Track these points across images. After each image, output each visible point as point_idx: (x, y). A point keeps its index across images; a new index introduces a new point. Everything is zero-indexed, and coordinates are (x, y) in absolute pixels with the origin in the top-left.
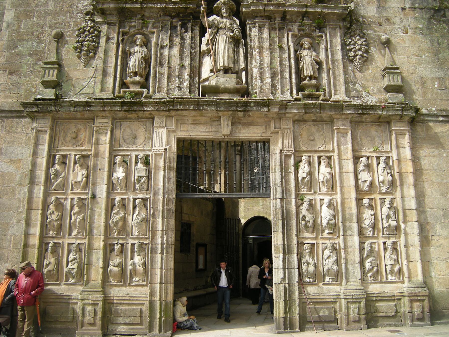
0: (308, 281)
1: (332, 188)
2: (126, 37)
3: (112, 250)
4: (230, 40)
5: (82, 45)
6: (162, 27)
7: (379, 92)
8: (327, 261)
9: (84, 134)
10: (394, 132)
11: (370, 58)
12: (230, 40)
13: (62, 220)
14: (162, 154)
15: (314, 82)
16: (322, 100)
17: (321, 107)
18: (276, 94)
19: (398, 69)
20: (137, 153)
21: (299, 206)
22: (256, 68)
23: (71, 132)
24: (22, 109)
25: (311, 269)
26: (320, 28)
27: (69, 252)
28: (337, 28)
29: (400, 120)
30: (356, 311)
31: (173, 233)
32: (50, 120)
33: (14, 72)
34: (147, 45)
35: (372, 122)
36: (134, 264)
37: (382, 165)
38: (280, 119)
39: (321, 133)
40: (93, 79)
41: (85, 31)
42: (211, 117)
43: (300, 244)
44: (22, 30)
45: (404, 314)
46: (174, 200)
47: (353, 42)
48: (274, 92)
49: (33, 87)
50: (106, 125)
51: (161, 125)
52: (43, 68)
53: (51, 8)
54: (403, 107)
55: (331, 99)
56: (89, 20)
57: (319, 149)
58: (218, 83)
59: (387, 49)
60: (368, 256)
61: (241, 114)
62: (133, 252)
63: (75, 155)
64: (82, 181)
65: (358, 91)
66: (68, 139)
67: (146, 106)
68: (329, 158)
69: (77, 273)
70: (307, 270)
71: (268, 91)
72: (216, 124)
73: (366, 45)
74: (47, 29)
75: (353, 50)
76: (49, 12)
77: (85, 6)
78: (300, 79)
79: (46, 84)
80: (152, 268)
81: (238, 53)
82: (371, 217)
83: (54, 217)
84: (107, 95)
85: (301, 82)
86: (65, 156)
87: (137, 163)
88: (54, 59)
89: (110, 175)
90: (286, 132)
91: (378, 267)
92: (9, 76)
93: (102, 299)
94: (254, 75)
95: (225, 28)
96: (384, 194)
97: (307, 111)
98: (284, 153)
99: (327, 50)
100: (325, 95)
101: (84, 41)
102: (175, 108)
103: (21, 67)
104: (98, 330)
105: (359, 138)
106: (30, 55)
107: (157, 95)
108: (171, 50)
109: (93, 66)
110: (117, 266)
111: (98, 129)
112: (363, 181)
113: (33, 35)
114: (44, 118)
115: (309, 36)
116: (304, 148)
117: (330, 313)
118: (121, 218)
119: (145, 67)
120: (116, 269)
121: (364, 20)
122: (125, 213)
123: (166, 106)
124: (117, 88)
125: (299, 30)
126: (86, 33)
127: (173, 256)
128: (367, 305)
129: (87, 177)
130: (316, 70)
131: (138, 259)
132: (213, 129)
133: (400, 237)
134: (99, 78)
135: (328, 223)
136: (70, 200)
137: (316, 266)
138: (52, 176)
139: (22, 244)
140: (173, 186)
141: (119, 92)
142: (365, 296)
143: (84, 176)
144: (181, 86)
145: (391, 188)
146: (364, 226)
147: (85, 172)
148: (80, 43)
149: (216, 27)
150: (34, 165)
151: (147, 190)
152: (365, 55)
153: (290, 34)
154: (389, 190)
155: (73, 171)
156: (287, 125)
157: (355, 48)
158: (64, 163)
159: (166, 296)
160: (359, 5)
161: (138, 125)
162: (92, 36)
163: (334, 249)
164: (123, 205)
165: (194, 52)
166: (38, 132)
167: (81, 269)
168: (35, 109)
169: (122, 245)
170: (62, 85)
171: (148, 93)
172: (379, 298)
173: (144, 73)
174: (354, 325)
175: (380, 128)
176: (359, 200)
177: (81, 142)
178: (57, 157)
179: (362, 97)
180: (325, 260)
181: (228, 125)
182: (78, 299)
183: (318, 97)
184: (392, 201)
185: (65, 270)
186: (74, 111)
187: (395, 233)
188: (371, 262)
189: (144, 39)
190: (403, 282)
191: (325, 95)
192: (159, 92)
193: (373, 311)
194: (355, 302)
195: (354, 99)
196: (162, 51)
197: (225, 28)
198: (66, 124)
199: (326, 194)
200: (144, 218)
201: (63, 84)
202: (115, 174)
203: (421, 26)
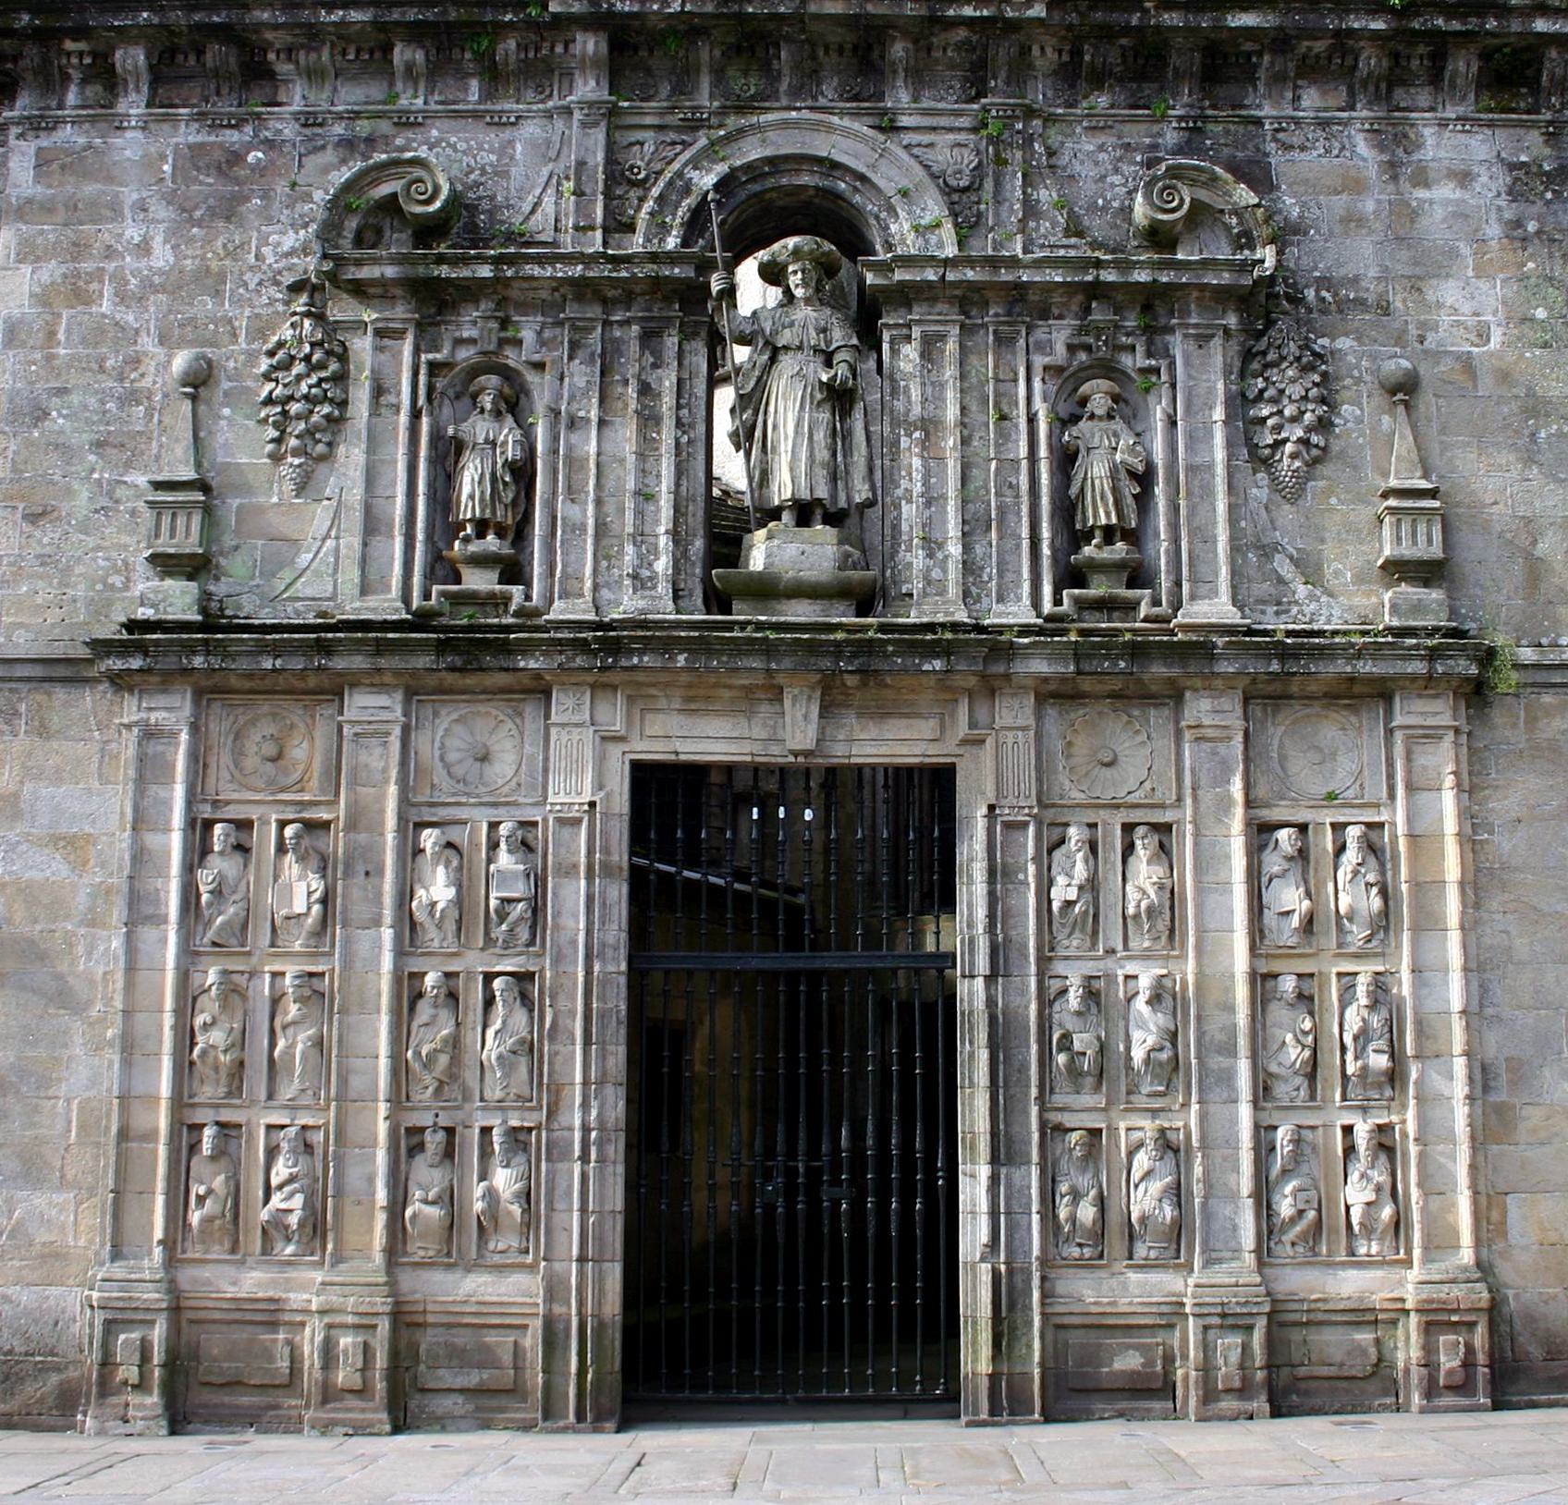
2: (440, 384)
4: (819, 396)
5: (285, 413)
6: (574, 346)
7: (1360, 579)
9: (305, 745)
10: (1399, 737)
11: (1336, 447)
12: (819, 396)
13: (243, 1049)
14: (580, 821)
15: (1120, 549)
16: (1144, 621)
17: (1139, 651)
18: (978, 600)
19: (1433, 493)
20: (494, 814)
21: (1051, 1003)
22: (910, 501)
23: (258, 738)
24: (84, 652)
25: (1087, 1213)
26: (1153, 333)
27: (272, 1153)
28: (1213, 336)
30: (1235, 1357)
31: (622, 1091)
32: (189, 696)
33: (44, 514)
34: (517, 403)
35: (1326, 695)
36: (491, 1195)
37: (1351, 856)
38: (992, 693)
40: (330, 543)
41: (293, 358)
42: (748, 690)
43: (1053, 1131)
44: (62, 352)
45: (1407, 1371)
46: (623, 980)
47: (1270, 393)
48: (974, 590)
49: (118, 572)
50: (386, 716)
51: (576, 719)
52: (152, 504)
53: (161, 263)
54: (1432, 649)
55: (1180, 619)
56: (308, 314)
57: (1130, 799)
58: (772, 564)
59: (1401, 409)
60: (1285, 1172)
61: (851, 681)
62: (486, 1152)
63: (282, 824)
64: (307, 914)
65: (1281, 581)
66: (251, 762)
67: (524, 653)
68: (1163, 829)
69: (301, 1224)
70: (1073, 1219)
71: (953, 591)
72: (765, 708)
73: (1323, 401)
74: (148, 343)
75: (1270, 422)
76: (157, 279)
77: (287, 255)
78: (1072, 531)
79: (165, 564)
80: (551, 1208)
81: (847, 436)
83: (217, 1037)
84: (387, 605)
85: (1077, 548)
86: (244, 825)
87: (493, 846)
88: (188, 474)
89: (405, 895)
90: (1010, 741)
91: (1319, 1210)
92: (27, 528)
93: (387, 1309)
94: (905, 527)
95: (800, 348)
96: (1357, 956)
97: (1086, 667)
98: (1005, 814)
99: (1173, 423)
100: (1156, 602)
101: (291, 398)
102: (624, 663)
103: (69, 492)
104: (375, 1410)
106: (99, 445)
107: (559, 611)
108: (607, 432)
109: (328, 492)
110: (433, 1203)
111: (358, 729)
113: (102, 369)
114: (165, 691)
115: (1108, 370)
116: (1077, 796)
117: (1149, 1363)
118: (445, 1040)
119: (514, 503)
120: (434, 1212)
121: (1324, 293)
122: (458, 1025)
123: (594, 653)
124: (417, 579)
125: (1071, 349)
126: (299, 368)
127: (620, 1169)
128: (1271, 1343)
129: (324, 901)
130: (1130, 500)
131: (504, 1179)
132: (758, 732)
133: (1404, 1107)
134: (351, 542)
135: (1147, 1061)
136: (267, 978)
137: (1101, 1202)
138: (205, 898)
139: (114, 1129)
140: (616, 932)
141: (427, 596)
142: (1267, 1309)
143: (317, 895)
144: (645, 573)
146: (1273, 1068)
147: (317, 884)
148: (279, 409)
149: (767, 343)
150: (141, 858)
151: (532, 942)
152: (1315, 439)
153: (1039, 361)
154: (1374, 943)
155: (276, 878)
156: (1014, 713)
157: (1280, 412)
158: (242, 849)
159: (599, 1303)
160: (1306, 233)
161: (494, 712)
162: (321, 380)
163: (1167, 1146)
165: (689, 441)
166: (150, 734)
167: (314, 1213)
168: (136, 663)
169: (450, 1131)
170: (217, 566)
171: (528, 597)
172: (1320, 1317)
173: (510, 521)
174: (1228, 1404)
175: (1353, 719)
176: (1262, 981)
177: (296, 776)
178: (218, 829)
179: (1296, 602)
180: (1136, 1186)
181: (806, 717)
182: (307, 1312)
184: (1380, 988)
185: (264, 1215)
186: (274, 670)
187: (1388, 1092)
188: (1295, 1193)
189: (507, 390)
190: (1408, 1263)
191: (1156, 602)
192: (565, 595)
193: (1296, 1358)
194: (1234, 1327)
195: (1263, 612)
196: (574, 438)
197: (800, 348)
198: (241, 710)
199: (1146, 956)
200: (522, 1041)
201: (223, 561)
202: (420, 893)
203: (1541, 313)
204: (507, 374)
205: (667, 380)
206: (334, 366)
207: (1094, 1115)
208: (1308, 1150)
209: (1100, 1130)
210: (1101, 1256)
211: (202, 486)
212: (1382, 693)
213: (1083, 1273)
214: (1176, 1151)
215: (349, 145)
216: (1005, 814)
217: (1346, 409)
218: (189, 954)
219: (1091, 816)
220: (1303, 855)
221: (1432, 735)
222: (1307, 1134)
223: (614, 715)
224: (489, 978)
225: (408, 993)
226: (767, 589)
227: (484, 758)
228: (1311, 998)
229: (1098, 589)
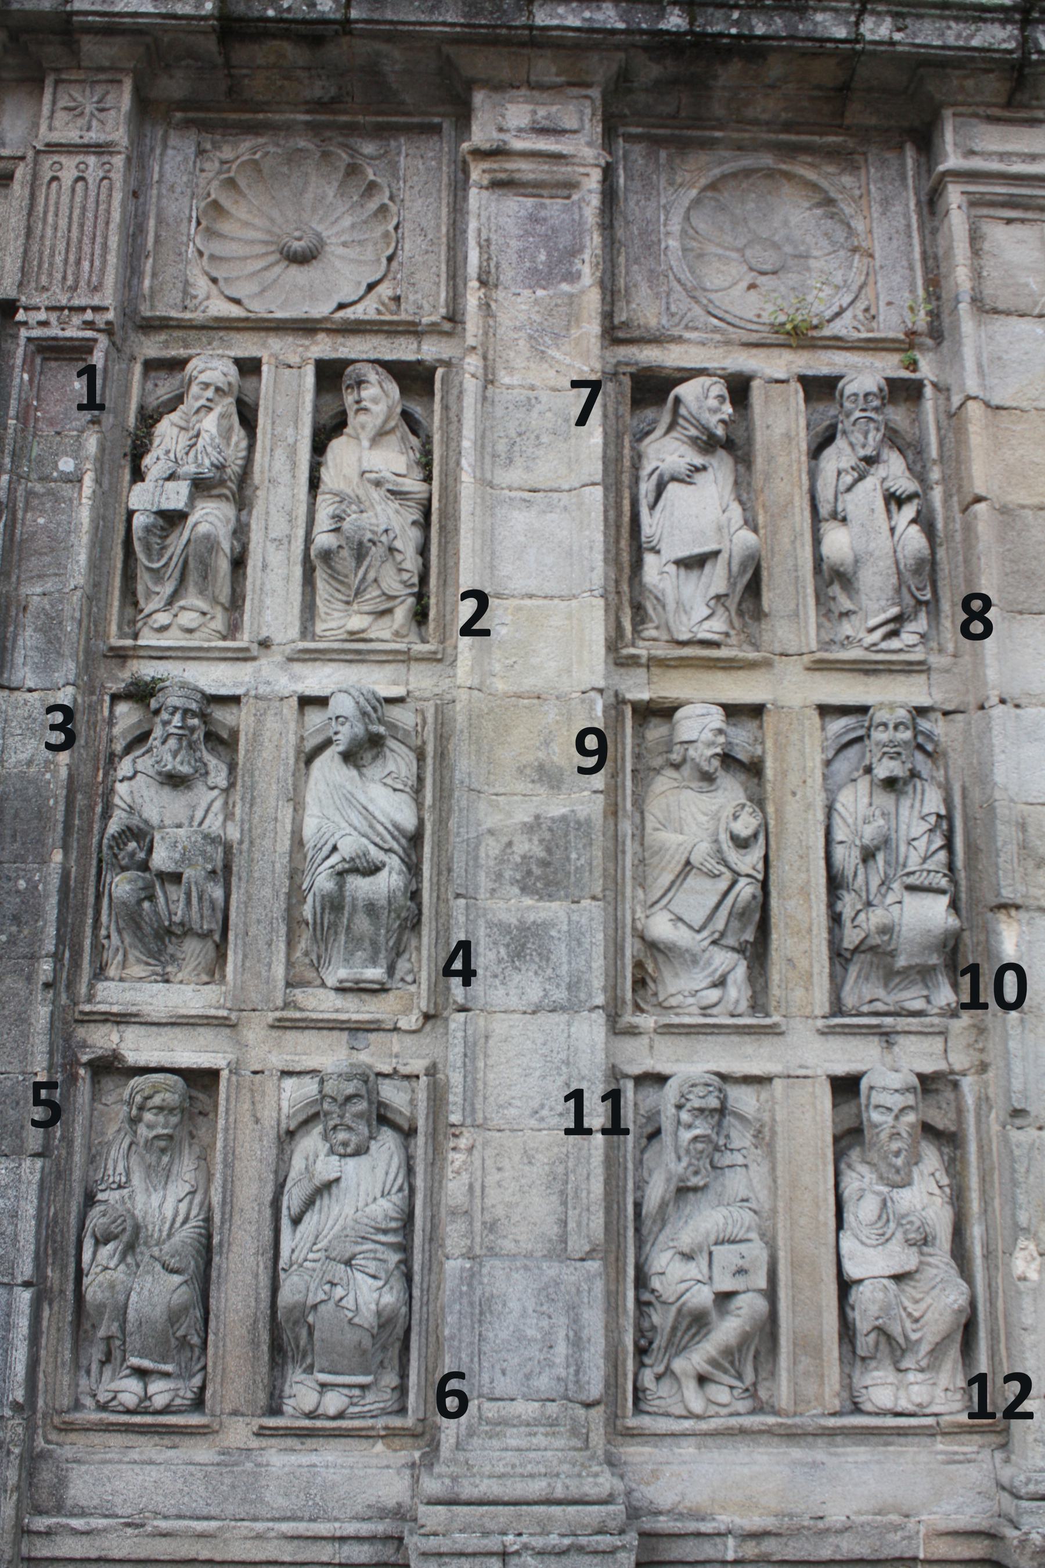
0: (129, 1399)
1: (420, 616)
8: (310, 1221)
10: (954, 195)
29: (1009, 105)
39: (373, 205)
82: (733, 855)
90: (68, 176)
91: (771, 1294)
105: (674, 243)
112: (680, 563)
145: (921, 624)
154: (908, 637)
175: (847, 180)
180: (296, 1221)
187: (945, 996)
207: (206, 1035)
208: (740, 1138)
209: (213, 1074)
210: (198, 1403)
213: (147, 1448)
214: (408, 1133)
219: (247, 346)
222: (744, 1099)
228: (754, 769)
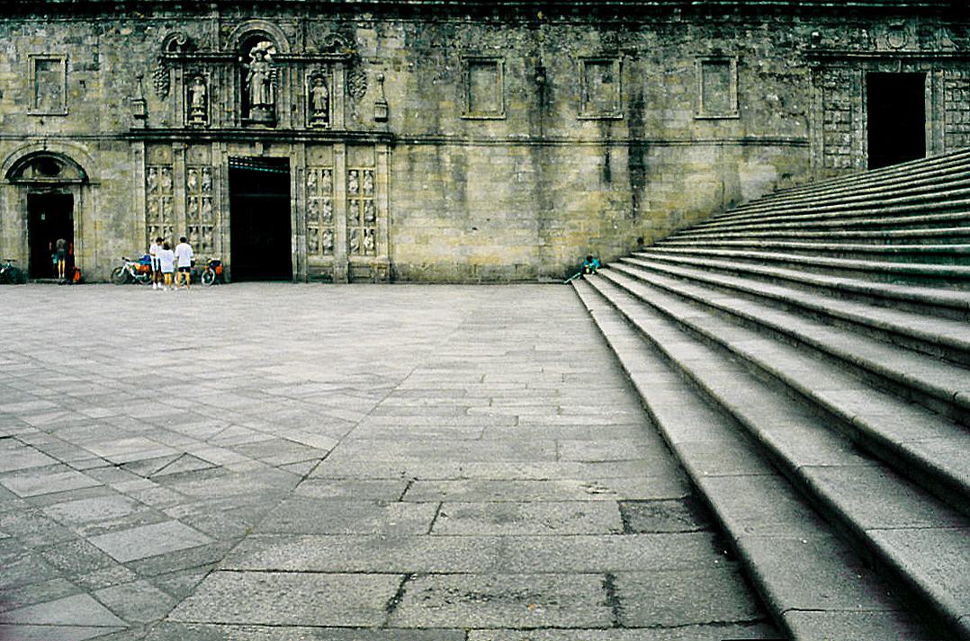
3: (191, 231)
79: (137, 117)
86: (156, 169)
88: (140, 98)
89: (186, 182)
98: (299, 168)
106: (123, 91)
115: (321, 76)
124: (186, 121)
129: (172, 183)
158: (156, 173)
164: (196, 201)
183: (324, 126)
204: (201, 76)
205: (232, 78)
206: (167, 75)
211: (143, 100)
212: (373, 144)
215: (167, 27)
216: (299, 168)
217: (370, 85)
218: (147, 195)
220: (358, 175)
221: (383, 153)
223: (224, 147)
224: (203, 198)
225: (188, 201)
226: (254, 122)
227: (201, 155)
229: (317, 123)
